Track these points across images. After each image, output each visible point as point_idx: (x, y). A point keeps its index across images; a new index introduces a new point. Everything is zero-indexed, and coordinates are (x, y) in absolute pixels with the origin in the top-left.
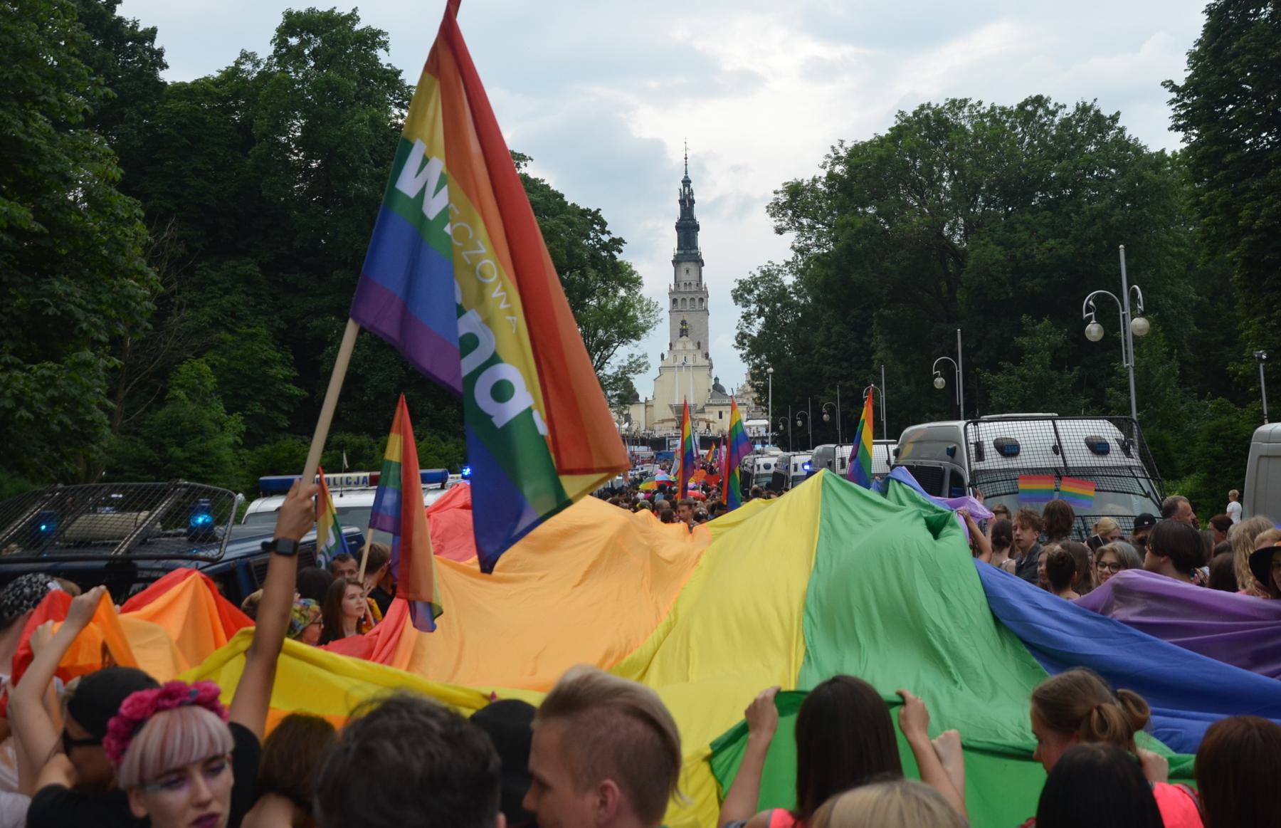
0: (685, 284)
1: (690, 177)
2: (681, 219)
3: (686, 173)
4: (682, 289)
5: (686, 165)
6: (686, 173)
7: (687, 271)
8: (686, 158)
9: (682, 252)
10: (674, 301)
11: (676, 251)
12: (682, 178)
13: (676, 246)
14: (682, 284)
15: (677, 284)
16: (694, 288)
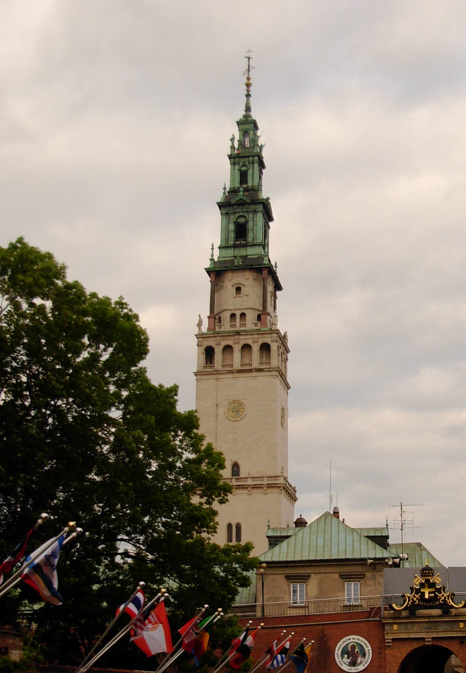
0: (233, 316)
1: (254, 115)
2: (233, 191)
3: (248, 109)
4: (226, 326)
5: (248, 96)
6: (248, 109)
7: (238, 290)
8: (248, 85)
9: (230, 253)
10: (209, 353)
11: (217, 253)
12: (240, 114)
13: (218, 243)
14: (226, 316)
15: (215, 317)
16: (250, 322)
